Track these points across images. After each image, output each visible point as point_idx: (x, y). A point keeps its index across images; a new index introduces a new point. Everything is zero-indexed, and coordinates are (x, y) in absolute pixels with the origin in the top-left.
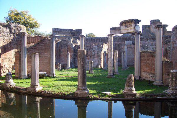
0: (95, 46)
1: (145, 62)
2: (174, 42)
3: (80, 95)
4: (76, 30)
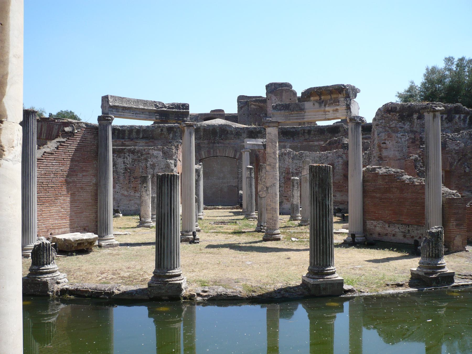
0: (155, 153)
1: (378, 195)
2: (382, 145)
3: (325, 289)
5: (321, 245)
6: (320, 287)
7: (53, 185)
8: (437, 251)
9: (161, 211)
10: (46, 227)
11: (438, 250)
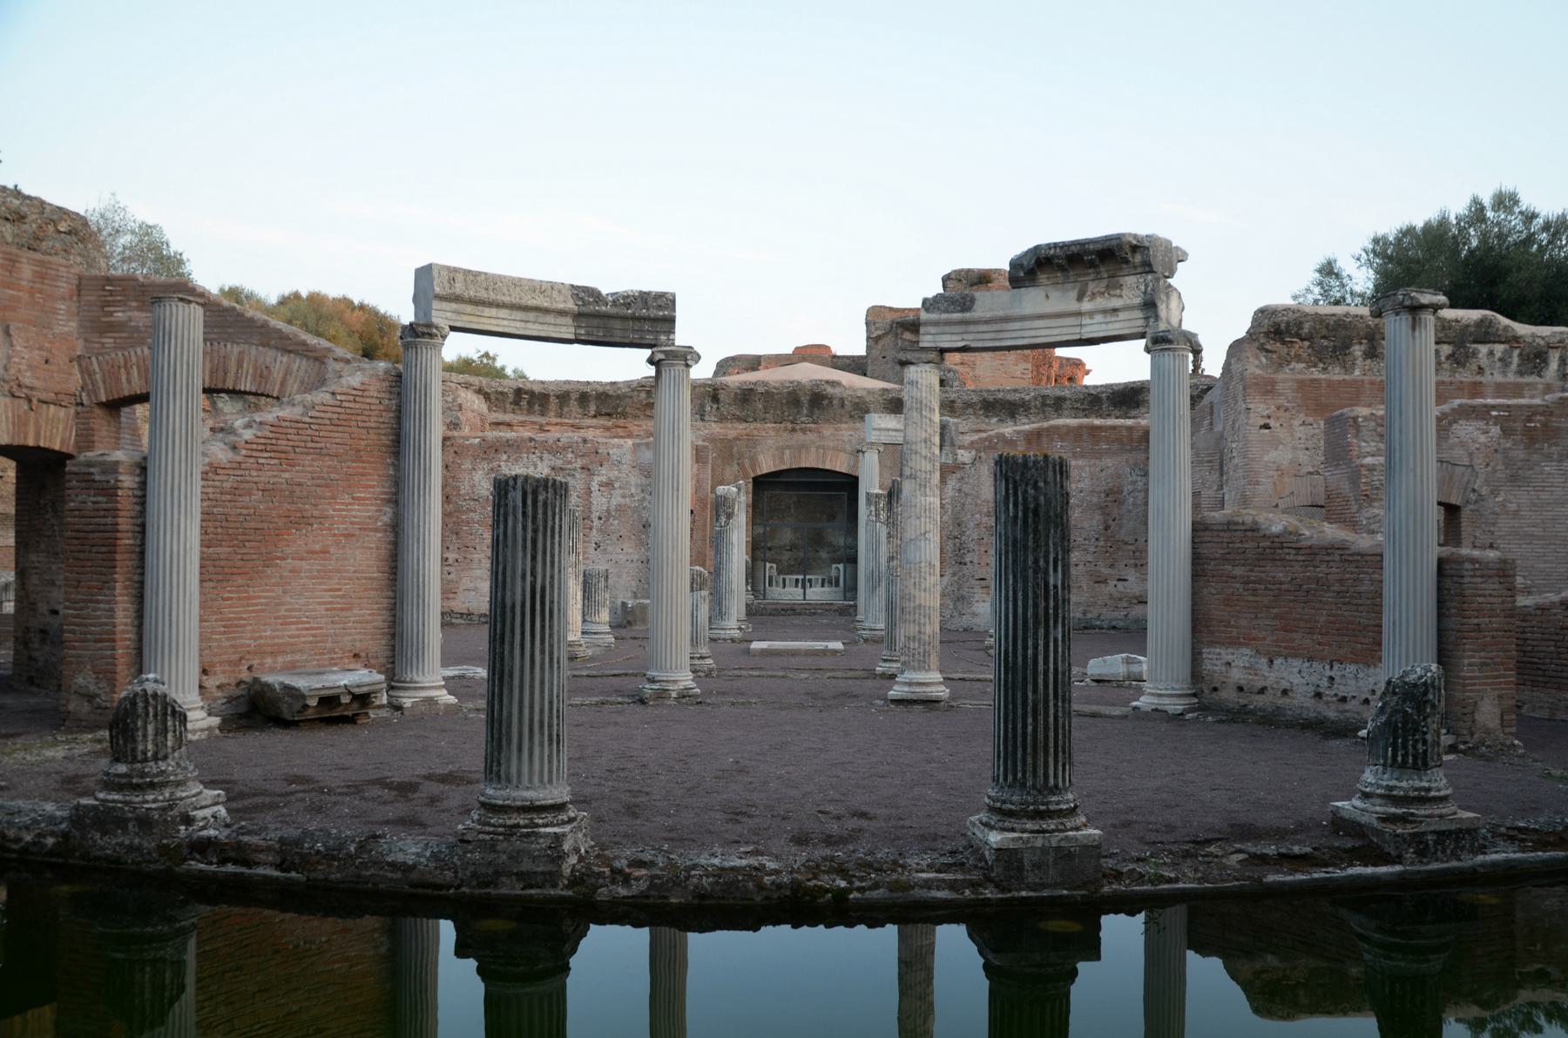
1: (1238, 571)
3: (1037, 866)
4: (627, 300)
5: (1030, 720)
6: (1021, 861)
7: (260, 526)
8: (1420, 746)
9: (503, 598)
10: (232, 646)
11: (1425, 742)
